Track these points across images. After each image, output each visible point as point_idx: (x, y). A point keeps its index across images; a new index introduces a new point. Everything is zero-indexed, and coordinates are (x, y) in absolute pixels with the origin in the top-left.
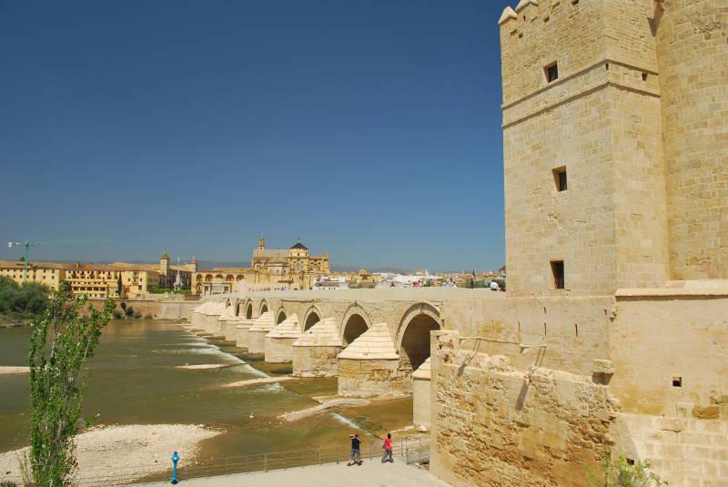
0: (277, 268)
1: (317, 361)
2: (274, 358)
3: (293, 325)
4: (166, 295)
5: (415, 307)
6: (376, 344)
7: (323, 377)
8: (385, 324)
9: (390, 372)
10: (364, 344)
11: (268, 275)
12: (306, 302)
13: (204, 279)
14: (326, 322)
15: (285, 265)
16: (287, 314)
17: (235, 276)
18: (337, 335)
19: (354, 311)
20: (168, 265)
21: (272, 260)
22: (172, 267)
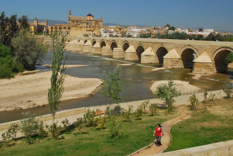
0: (84, 25)
1: (173, 63)
2: (145, 62)
3: (150, 51)
4: (43, 36)
5: (223, 47)
6: (205, 58)
7: (174, 68)
8: (206, 52)
9: (210, 66)
10: (202, 58)
11: (81, 28)
12: (158, 43)
13: (54, 29)
14: (174, 51)
15: (87, 24)
16: (144, 47)
17: (67, 28)
18: (178, 55)
19: (188, 47)
20: (37, 23)
21: (82, 21)
22: (39, 24)
